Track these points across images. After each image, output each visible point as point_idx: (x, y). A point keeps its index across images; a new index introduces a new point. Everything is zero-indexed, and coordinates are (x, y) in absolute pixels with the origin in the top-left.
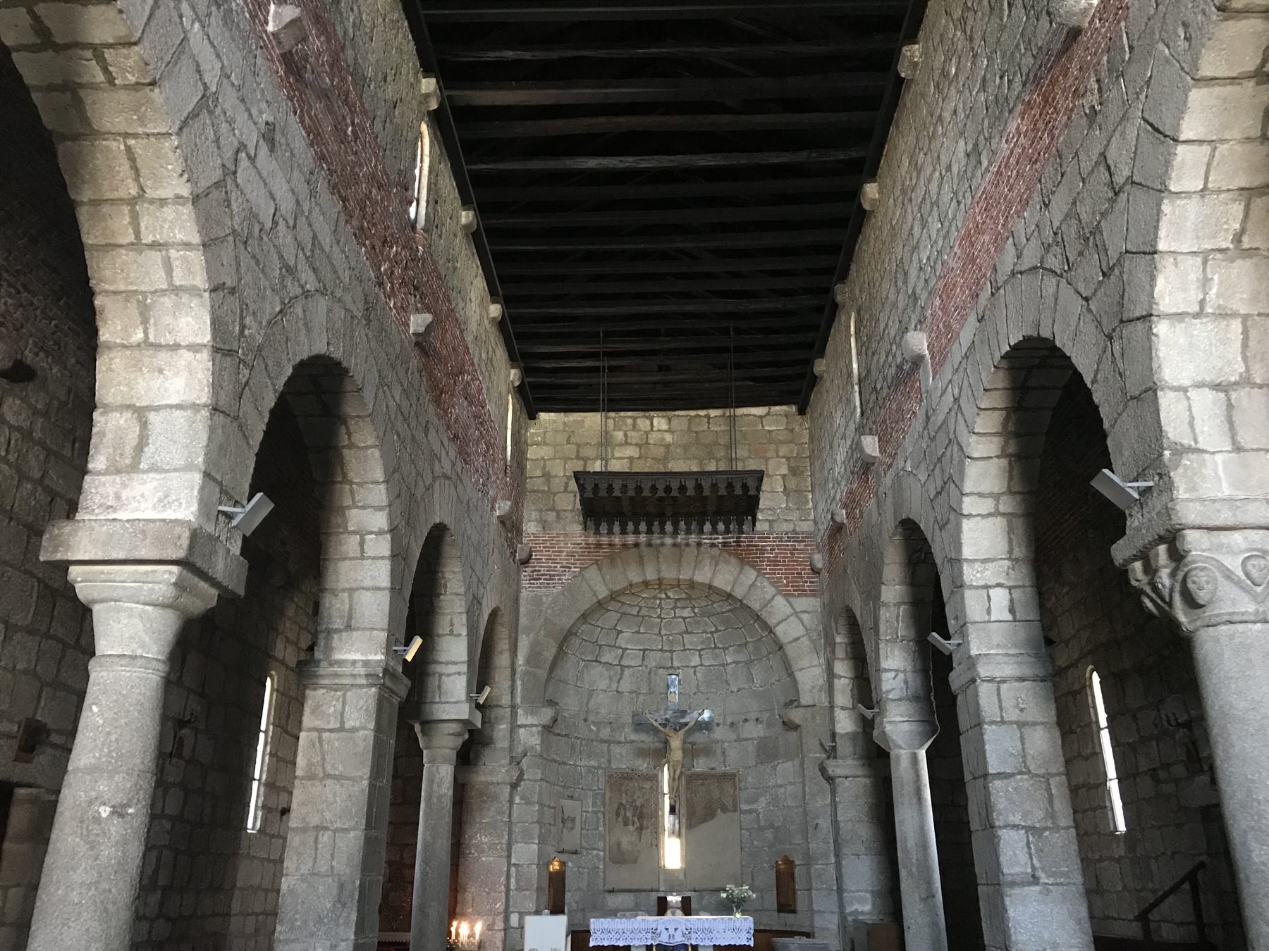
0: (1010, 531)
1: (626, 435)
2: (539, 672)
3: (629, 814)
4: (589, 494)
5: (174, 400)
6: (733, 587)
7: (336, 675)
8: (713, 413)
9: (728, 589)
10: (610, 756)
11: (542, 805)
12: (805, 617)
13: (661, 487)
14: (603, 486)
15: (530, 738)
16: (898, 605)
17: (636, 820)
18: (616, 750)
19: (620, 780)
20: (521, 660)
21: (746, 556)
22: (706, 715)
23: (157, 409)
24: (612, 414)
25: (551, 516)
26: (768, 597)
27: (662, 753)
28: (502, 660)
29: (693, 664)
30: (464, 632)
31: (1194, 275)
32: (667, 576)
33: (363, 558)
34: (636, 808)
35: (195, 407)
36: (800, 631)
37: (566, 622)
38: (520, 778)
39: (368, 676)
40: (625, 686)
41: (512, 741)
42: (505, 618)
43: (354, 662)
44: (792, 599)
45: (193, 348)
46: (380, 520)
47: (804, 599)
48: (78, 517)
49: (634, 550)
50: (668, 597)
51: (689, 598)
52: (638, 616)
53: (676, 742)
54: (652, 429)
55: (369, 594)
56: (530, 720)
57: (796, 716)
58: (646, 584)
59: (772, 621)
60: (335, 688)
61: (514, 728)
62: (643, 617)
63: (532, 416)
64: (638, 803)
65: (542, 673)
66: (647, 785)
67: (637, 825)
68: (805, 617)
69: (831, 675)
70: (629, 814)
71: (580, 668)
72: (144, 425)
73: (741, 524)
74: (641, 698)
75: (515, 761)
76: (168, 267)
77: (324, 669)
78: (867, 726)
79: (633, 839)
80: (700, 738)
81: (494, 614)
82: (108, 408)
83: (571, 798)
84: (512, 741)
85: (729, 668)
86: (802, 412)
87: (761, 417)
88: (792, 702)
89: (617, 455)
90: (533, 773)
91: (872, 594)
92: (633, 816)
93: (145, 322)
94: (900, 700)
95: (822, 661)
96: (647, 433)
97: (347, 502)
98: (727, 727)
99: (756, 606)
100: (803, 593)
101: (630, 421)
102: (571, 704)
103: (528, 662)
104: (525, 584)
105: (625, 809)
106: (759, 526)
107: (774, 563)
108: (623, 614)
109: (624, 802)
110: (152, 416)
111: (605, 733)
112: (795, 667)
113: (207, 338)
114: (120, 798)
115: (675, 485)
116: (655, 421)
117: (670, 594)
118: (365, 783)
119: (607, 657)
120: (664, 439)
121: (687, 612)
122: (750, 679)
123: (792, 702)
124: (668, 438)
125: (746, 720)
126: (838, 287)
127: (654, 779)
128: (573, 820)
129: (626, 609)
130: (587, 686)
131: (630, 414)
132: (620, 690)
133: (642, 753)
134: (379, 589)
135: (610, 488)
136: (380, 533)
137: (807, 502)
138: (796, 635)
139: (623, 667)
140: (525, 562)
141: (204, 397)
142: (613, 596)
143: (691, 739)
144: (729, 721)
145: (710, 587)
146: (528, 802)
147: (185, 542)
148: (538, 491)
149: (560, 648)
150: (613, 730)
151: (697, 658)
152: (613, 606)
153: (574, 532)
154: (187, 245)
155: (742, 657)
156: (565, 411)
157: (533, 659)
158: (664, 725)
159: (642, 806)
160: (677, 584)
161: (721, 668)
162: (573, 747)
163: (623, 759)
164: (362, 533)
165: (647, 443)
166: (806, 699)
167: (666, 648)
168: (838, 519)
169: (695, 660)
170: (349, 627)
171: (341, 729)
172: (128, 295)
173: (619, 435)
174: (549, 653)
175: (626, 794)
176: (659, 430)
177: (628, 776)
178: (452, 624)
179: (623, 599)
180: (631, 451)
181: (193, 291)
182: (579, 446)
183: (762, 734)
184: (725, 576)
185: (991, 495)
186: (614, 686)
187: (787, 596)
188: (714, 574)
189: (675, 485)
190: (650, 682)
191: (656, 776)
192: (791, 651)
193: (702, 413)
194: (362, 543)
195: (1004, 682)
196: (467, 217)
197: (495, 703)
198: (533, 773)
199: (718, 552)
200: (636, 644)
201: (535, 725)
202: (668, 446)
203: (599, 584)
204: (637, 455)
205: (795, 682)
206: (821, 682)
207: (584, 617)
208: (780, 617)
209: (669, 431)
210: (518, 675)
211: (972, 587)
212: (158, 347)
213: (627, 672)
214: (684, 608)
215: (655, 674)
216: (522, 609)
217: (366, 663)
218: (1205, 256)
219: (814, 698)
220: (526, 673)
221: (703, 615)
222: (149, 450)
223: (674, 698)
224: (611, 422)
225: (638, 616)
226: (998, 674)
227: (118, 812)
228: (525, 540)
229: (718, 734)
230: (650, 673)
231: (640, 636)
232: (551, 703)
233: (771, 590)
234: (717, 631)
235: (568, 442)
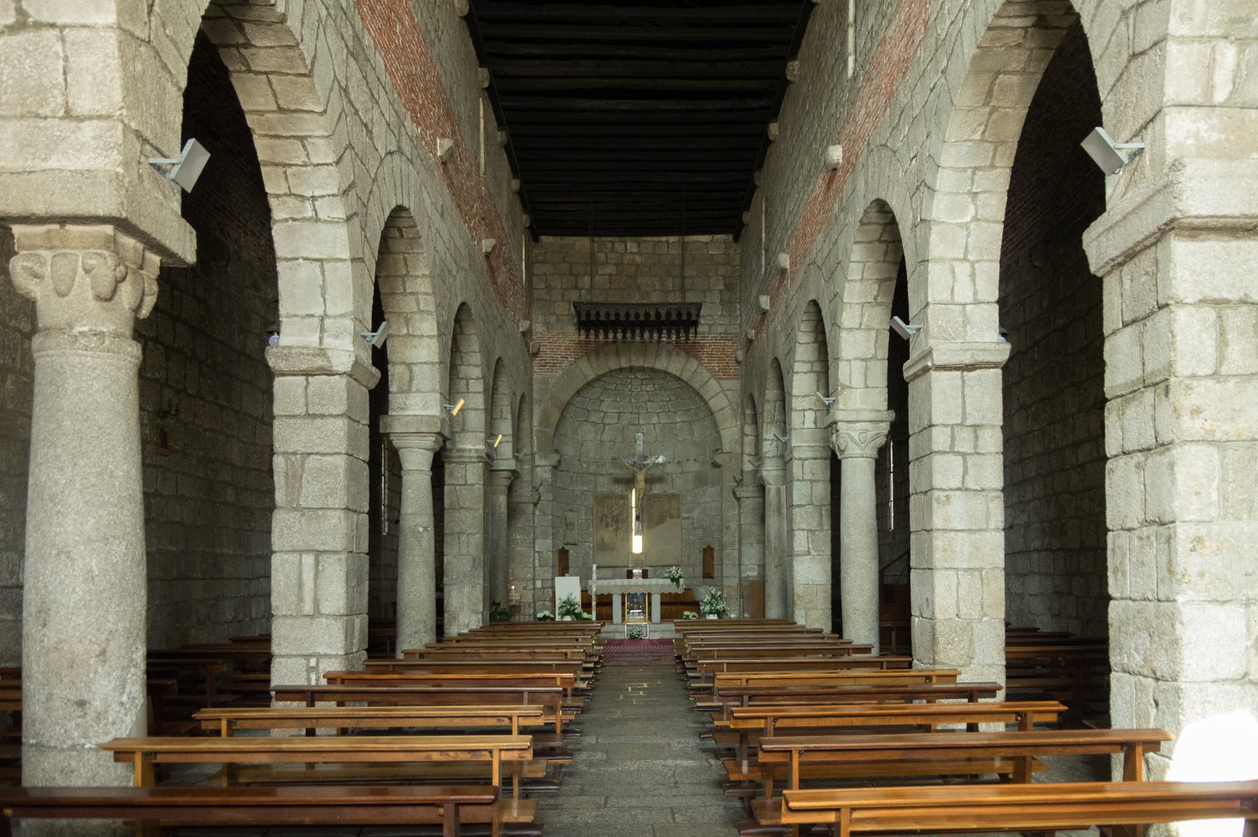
0: (818, 381)
1: (606, 256)
2: (549, 430)
4: (584, 318)
5: (423, 361)
7: (461, 457)
8: (672, 239)
9: (678, 375)
11: (553, 515)
12: (729, 393)
13: (632, 313)
14: (593, 313)
15: (543, 473)
16: (775, 401)
18: (600, 479)
19: (602, 499)
20: (535, 423)
21: (691, 350)
22: (661, 460)
23: (416, 364)
24: (596, 239)
25: (553, 319)
26: (705, 380)
27: (630, 482)
28: (525, 424)
30: (509, 417)
31: (858, 312)
33: (468, 392)
35: (432, 363)
36: (724, 403)
37: (565, 397)
38: (539, 499)
39: (478, 457)
40: (606, 437)
41: (532, 476)
42: (527, 399)
43: (470, 450)
44: (721, 381)
45: (429, 337)
46: (477, 372)
47: (729, 381)
48: (391, 413)
49: (614, 346)
50: (636, 378)
51: (651, 378)
53: (640, 477)
54: (626, 252)
55: (473, 412)
56: (543, 462)
58: (621, 370)
59: (707, 397)
60: (461, 463)
63: (536, 239)
64: (615, 513)
65: (551, 431)
66: (621, 502)
68: (729, 393)
72: (411, 371)
73: (687, 333)
74: (617, 445)
75: (536, 489)
76: (418, 304)
77: (454, 454)
78: (756, 472)
80: (657, 472)
81: (523, 396)
82: (394, 364)
83: (571, 511)
84: (532, 476)
85: (678, 425)
86: (736, 239)
87: (706, 243)
88: (718, 450)
89: (600, 272)
90: (547, 496)
91: (762, 395)
93: (407, 325)
95: (739, 423)
96: (622, 254)
97: (459, 362)
99: (696, 385)
100: (728, 377)
101: (609, 245)
102: (569, 450)
103: (540, 424)
104: (536, 369)
106: (700, 329)
107: (711, 355)
108: (606, 389)
110: (414, 367)
111: (593, 468)
112: (720, 427)
113: (435, 332)
114: (426, 525)
115: (642, 312)
116: (629, 245)
117: (638, 375)
118: (481, 511)
119: (593, 418)
120: (634, 260)
121: (650, 388)
122: (692, 433)
123: (718, 450)
124: (638, 259)
125: (688, 460)
126: (756, 174)
127: (626, 498)
128: (573, 524)
129: (609, 387)
131: (609, 239)
133: (617, 481)
134: (478, 409)
135: (598, 314)
136: (477, 379)
137: (736, 311)
138: (723, 406)
140: (535, 354)
141: (436, 359)
142: (598, 378)
143: (651, 472)
145: (666, 372)
146: (545, 514)
147: (439, 425)
148: (542, 300)
149: (562, 414)
150: (598, 466)
151: (656, 418)
153: (571, 334)
154: (426, 294)
156: (560, 235)
157: (544, 421)
158: (633, 466)
159: (618, 515)
160: (643, 370)
162: (571, 478)
163: (605, 486)
164: (467, 379)
165: (622, 263)
166: (726, 448)
167: (635, 411)
168: (749, 337)
169: (655, 420)
170: (463, 430)
171: (466, 484)
172: (400, 314)
173: (601, 256)
174: (555, 417)
176: (631, 253)
177: (608, 497)
178: (501, 412)
179: (605, 379)
180: (610, 270)
181: (429, 312)
182: (571, 264)
184: (674, 365)
185: (809, 362)
186: (598, 438)
187: (718, 379)
189: (642, 312)
192: (718, 416)
193: (663, 239)
194: (467, 385)
195: (806, 459)
196: (501, 136)
198: (547, 496)
202: (638, 266)
203: (589, 370)
204: (615, 273)
205: (720, 437)
206: (737, 437)
207: (578, 393)
208: (712, 393)
209: (639, 253)
210: (534, 433)
211: (796, 410)
212: (414, 336)
213: (607, 427)
216: (535, 387)
217: (477, 451)
218: (863, 305)
220: (540, 431)
221: (660, 389)
222: (415, 382)
223: (640, 447)
224: (596, 245)
226: (803, 456)
227: (425, 529)
228: (534, 337)
229: (669, 469)
232: (557, 451)
233: (707, 375)
234: (670, 400)
235: (564, 262)
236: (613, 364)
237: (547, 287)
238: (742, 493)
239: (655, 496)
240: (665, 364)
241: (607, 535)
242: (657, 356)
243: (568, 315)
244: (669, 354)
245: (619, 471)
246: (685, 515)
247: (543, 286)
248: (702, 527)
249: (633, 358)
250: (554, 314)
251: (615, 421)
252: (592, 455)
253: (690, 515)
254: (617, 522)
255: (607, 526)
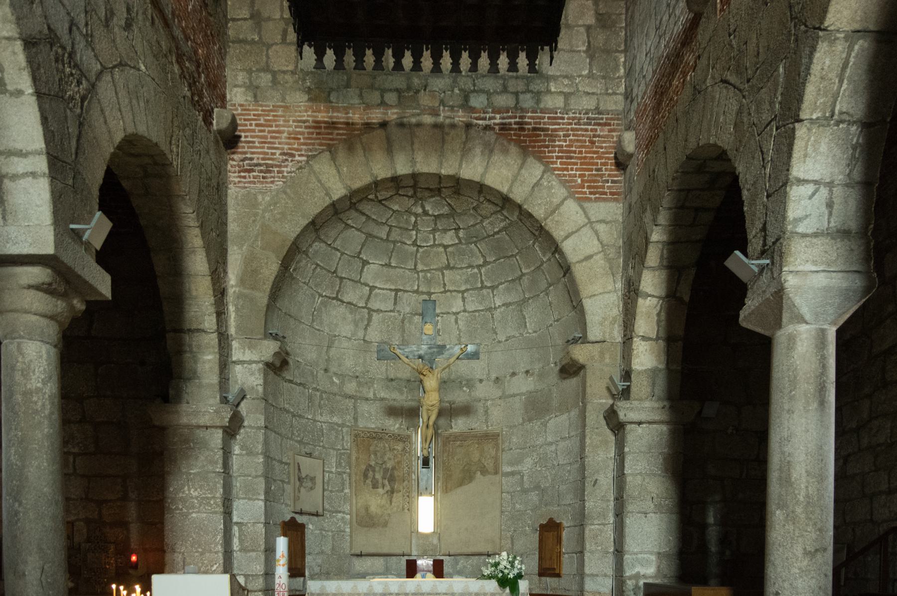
3: (378, 476)
6: (511, 187)
10: (356, 413)
17: (386, 482)
29: (454, 310)
32: (425, 169)
34: (386, 470)
52: (387, 240)
57: (580, 353)
61: (224, 364)
62: (394, 242)
64: (389, 465)
67: (388, 488)
69: (631, 293)
70: (378, 476)
71: (316, 305)
79: (383, 502)
92: (384, 478)
94: (816, 235)
98: (491, 383)
105: (374, 471)
109: (373, 463)
121: (449, 239)
130: (327, 330)
132: (366, 339)
139: (370, 310)
143: (450, 397)
144: (493, 376)
150: (360, 384)
152: (354, 218)
155: (512, 298)
159: (394, 468)
161: (488, 314)
175: (376, 455)
183: (531, 387)
188: (487, 168)
190: (404, 331)
191: (409, 437)
197: (194, 327)
199: (493, 137)
200: (387, 281)
201: (255, 362)
214: (445, 231)
215: (410, 322)
219: (604, 333)
225: (387, 240)
229: (481, 391)
230: (403, 321)
231: (392, 271)
236: (381, 169)
237: (252, 17)
238: (627, 412)
239: (457, 437)
240: (480, 170)
241: (375, 501)
242: (465, 152)
243: (293, 73)
244: (489, 150)
245: (395, 395)
246: (508, 469)
247: (245, 13)
248: (537, 487)
249: (419, 157)
250: (267, 69)
251: (390, 306)
252: (349, 363)
253: (519, 468)
254: (392, 479)
255: (375, 486)
